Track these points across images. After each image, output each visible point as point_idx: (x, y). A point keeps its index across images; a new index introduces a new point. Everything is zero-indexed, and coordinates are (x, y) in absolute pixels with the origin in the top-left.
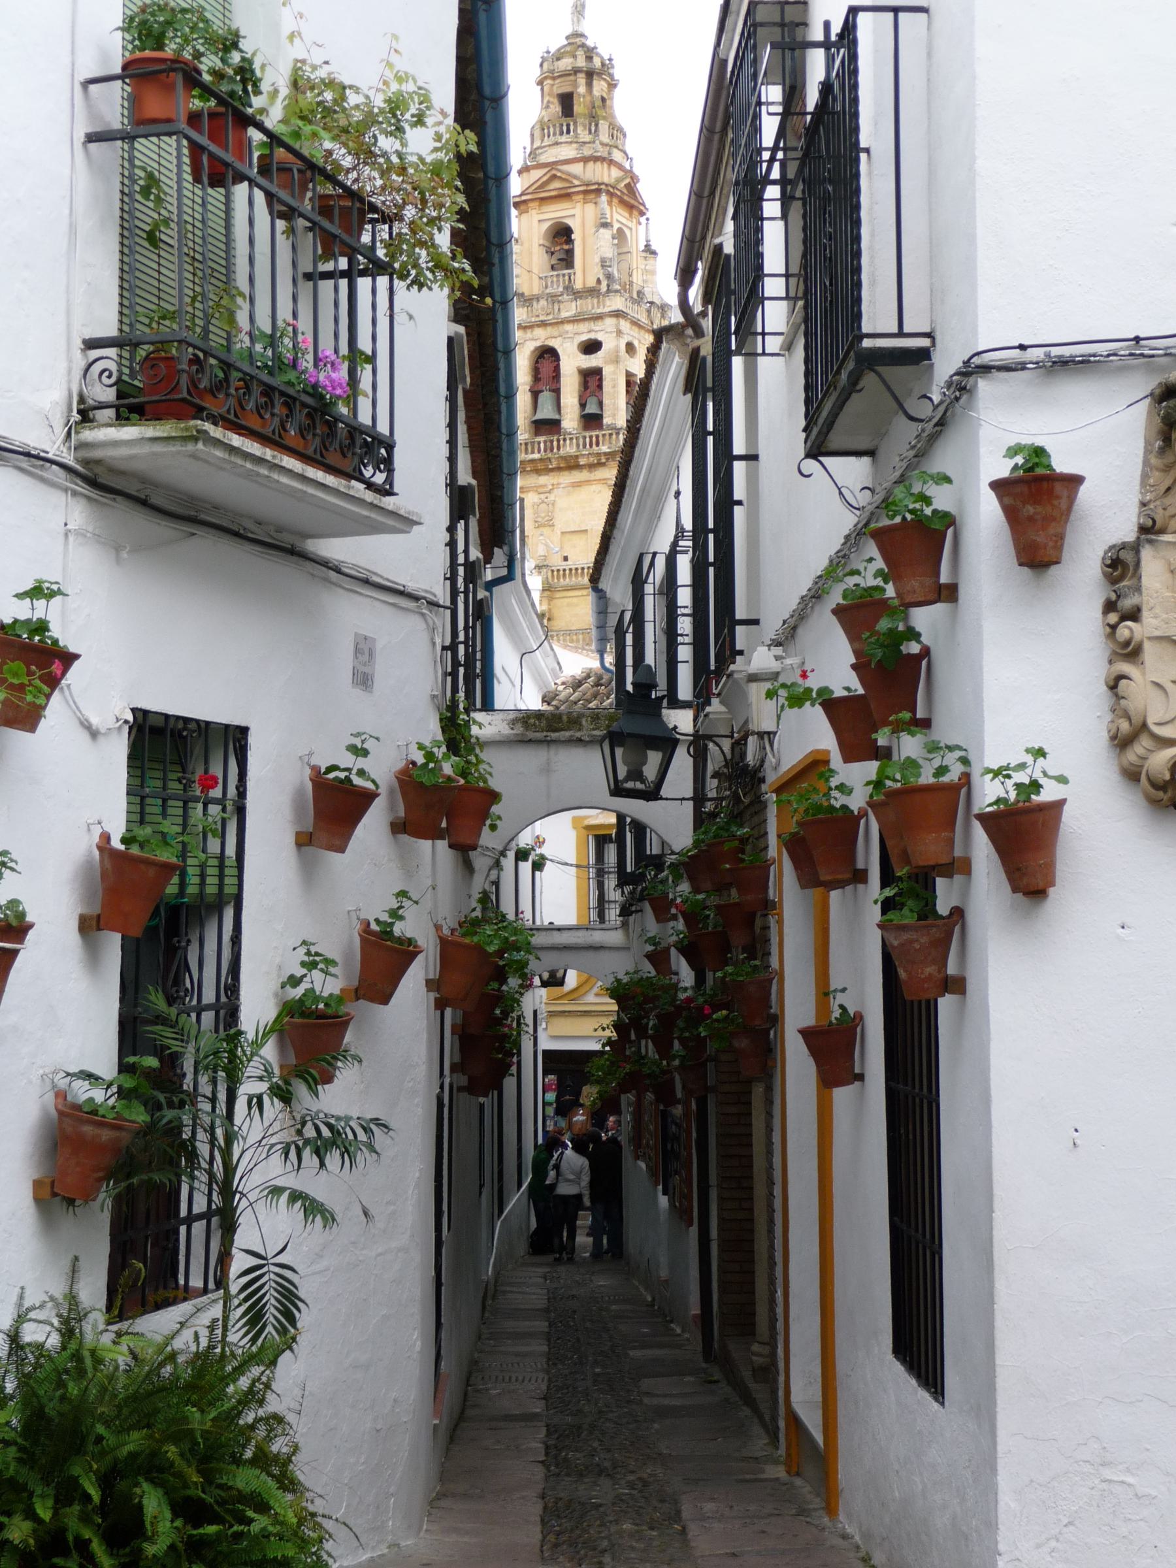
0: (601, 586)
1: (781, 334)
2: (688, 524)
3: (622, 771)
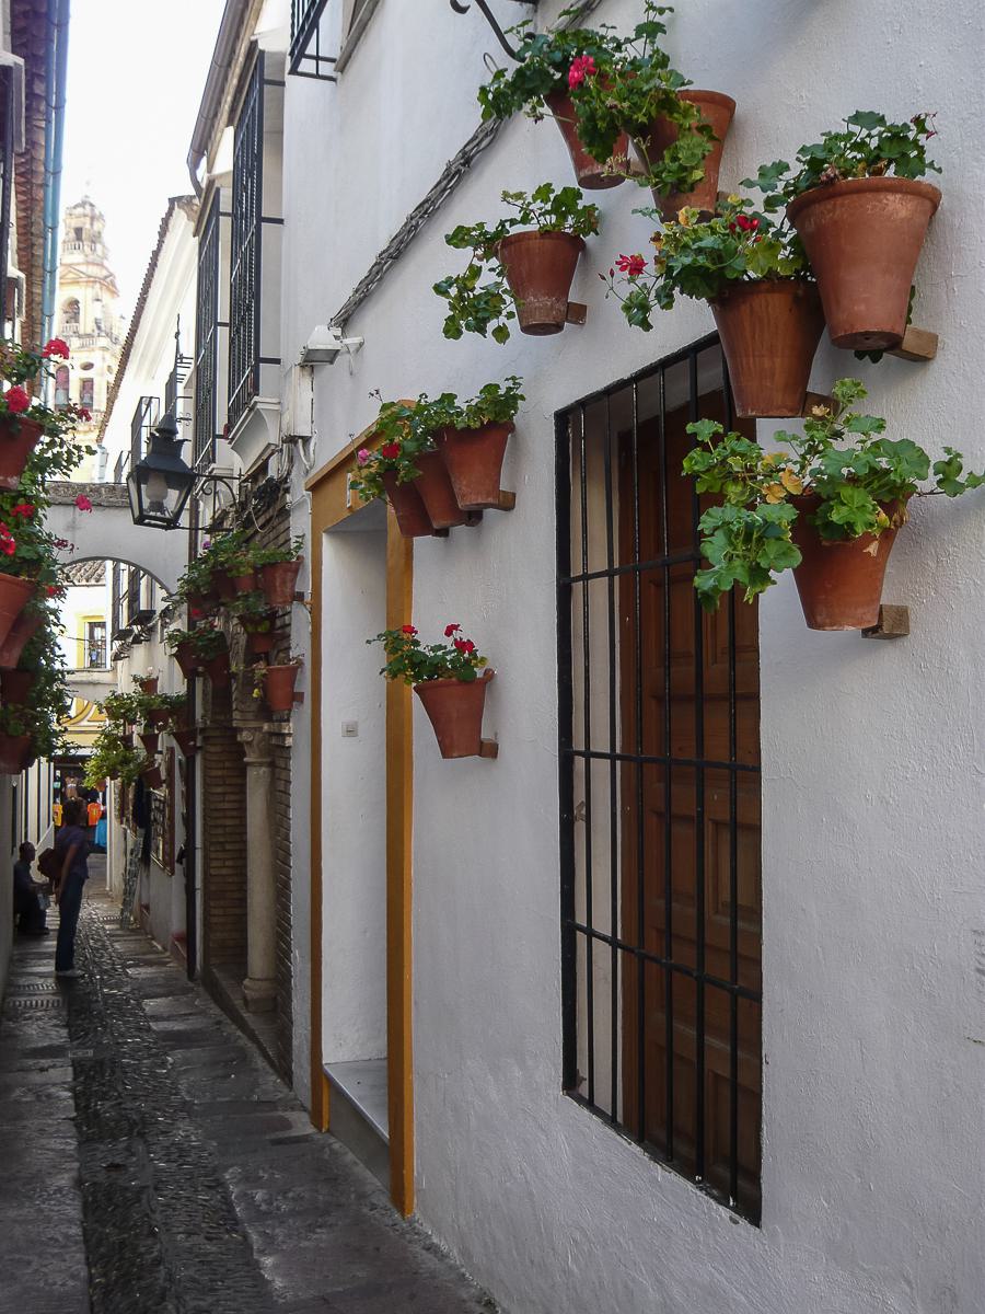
0: (103, 444)
1: (333, 60)
2: (188, 349)
3: (146, 503)
